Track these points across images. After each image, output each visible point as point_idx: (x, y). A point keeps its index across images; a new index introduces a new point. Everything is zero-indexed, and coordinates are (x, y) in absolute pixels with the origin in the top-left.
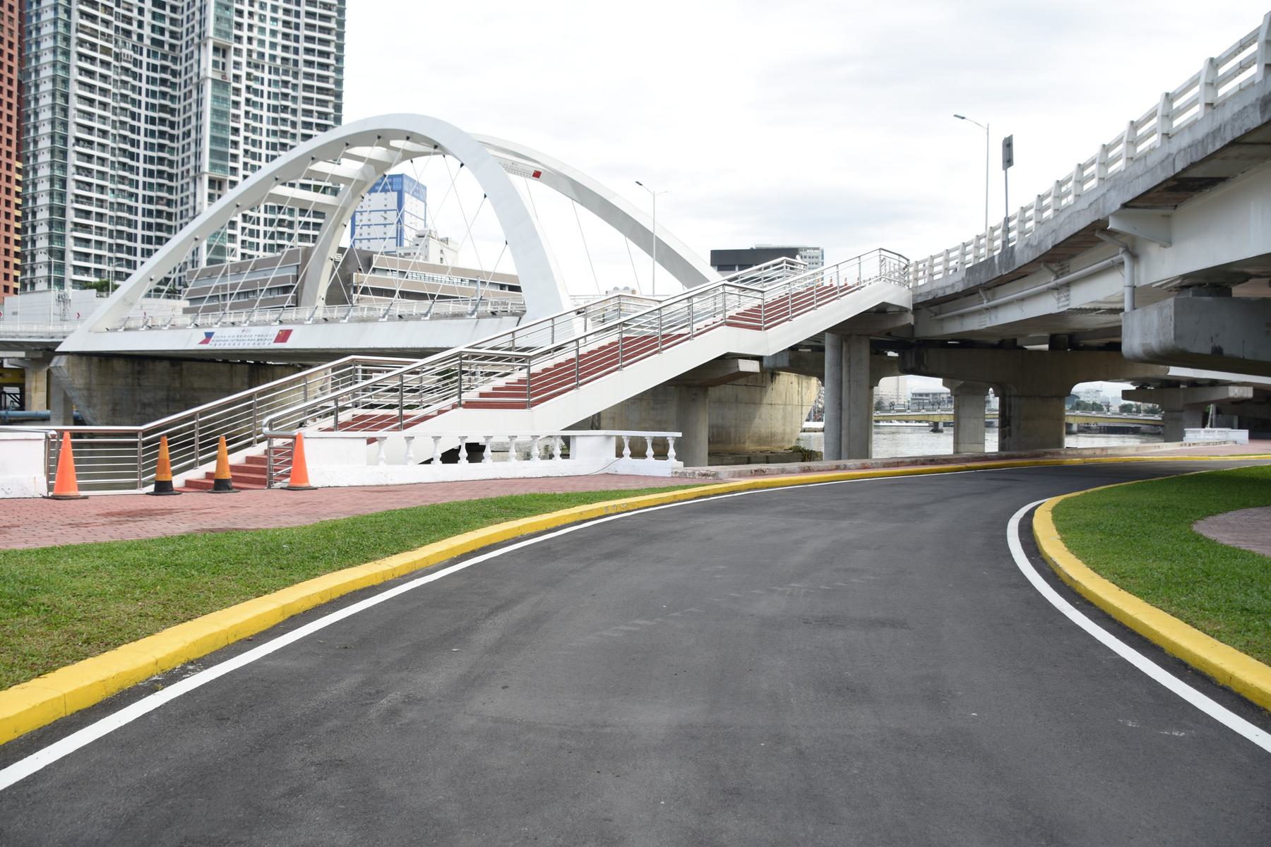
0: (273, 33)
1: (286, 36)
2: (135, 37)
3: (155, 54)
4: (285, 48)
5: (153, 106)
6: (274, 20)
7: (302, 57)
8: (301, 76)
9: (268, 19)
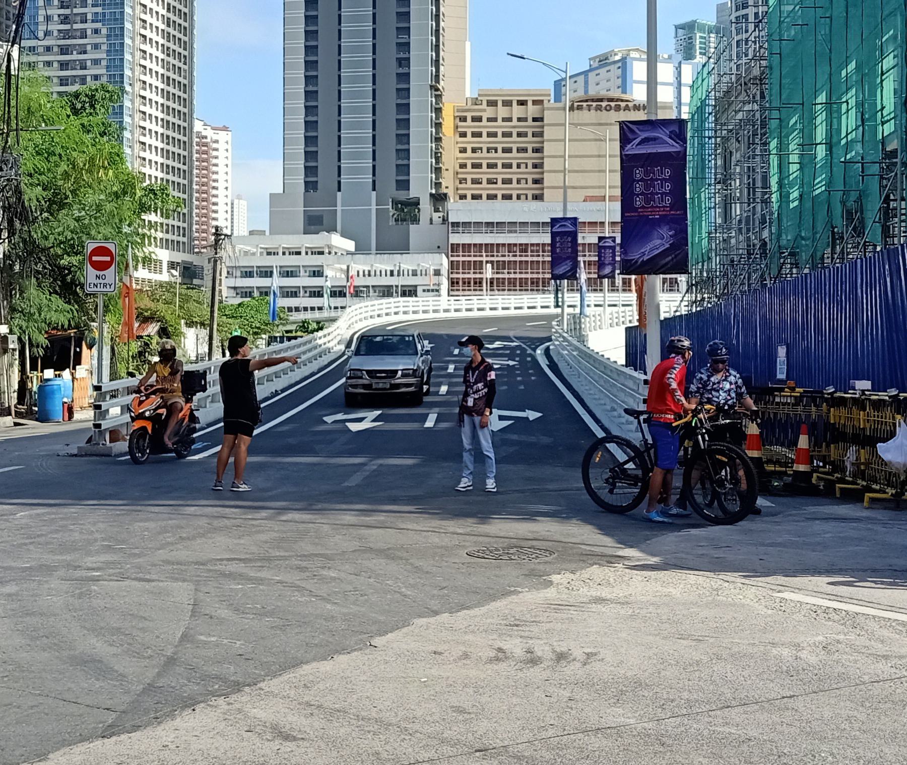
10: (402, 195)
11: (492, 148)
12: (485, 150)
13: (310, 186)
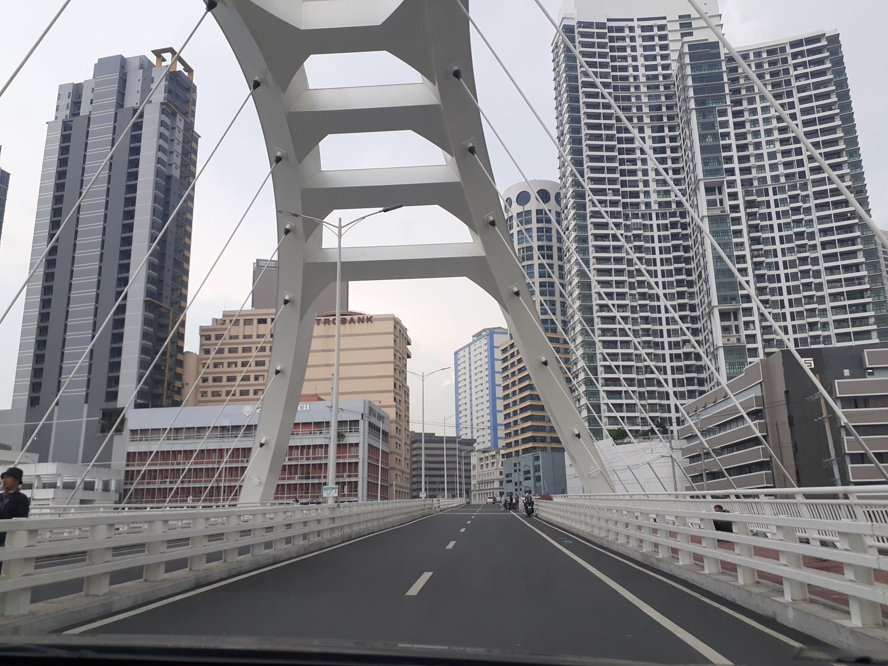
0: (772, 156)
2: (643, 207)
3: (664, 216)
4: (787, 165)
5: (668, 260)
6: (769, 143)
9: (764, 144)
10: (110, 405)
11: (233, 363)
12: (226, 365)
13: (34, 401)
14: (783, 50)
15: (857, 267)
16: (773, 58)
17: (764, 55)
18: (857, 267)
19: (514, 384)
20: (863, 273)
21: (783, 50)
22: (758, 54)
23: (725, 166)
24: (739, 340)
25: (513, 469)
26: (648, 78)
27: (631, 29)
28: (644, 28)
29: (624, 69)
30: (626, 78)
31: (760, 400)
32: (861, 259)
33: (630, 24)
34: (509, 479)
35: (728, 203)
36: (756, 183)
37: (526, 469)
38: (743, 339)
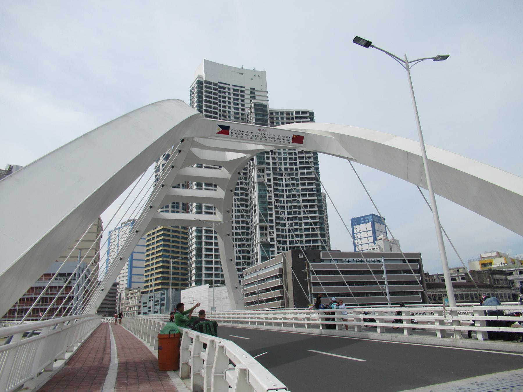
0: (285, 159)
1: (291, 159)
4: (291, 164)
6: (284, 153)
7: (298, 166)
8: (299, 174)
9: (282, 153)
14: (292, 114)
15: (314, 212)
16: (288, 116)
17: (285, 115)
18: (314, 212)
19: (153, 254)
20: (317, 215)
21: (292, 114)
22: (282, 113)
23: (266, 161)
24: (267, 240)
25: (148, 299)
26: (235, 113)
27: (229, 89)
28: (234, 90)
29: (224, 107)
30: (225, 111)
31: (281, 270)
32: (316, 209)
33: (229, 86)
34: (145, 305)
35: (266, 178)
36: (278, 170)
37: (156, 299)
38: (269, 239)
